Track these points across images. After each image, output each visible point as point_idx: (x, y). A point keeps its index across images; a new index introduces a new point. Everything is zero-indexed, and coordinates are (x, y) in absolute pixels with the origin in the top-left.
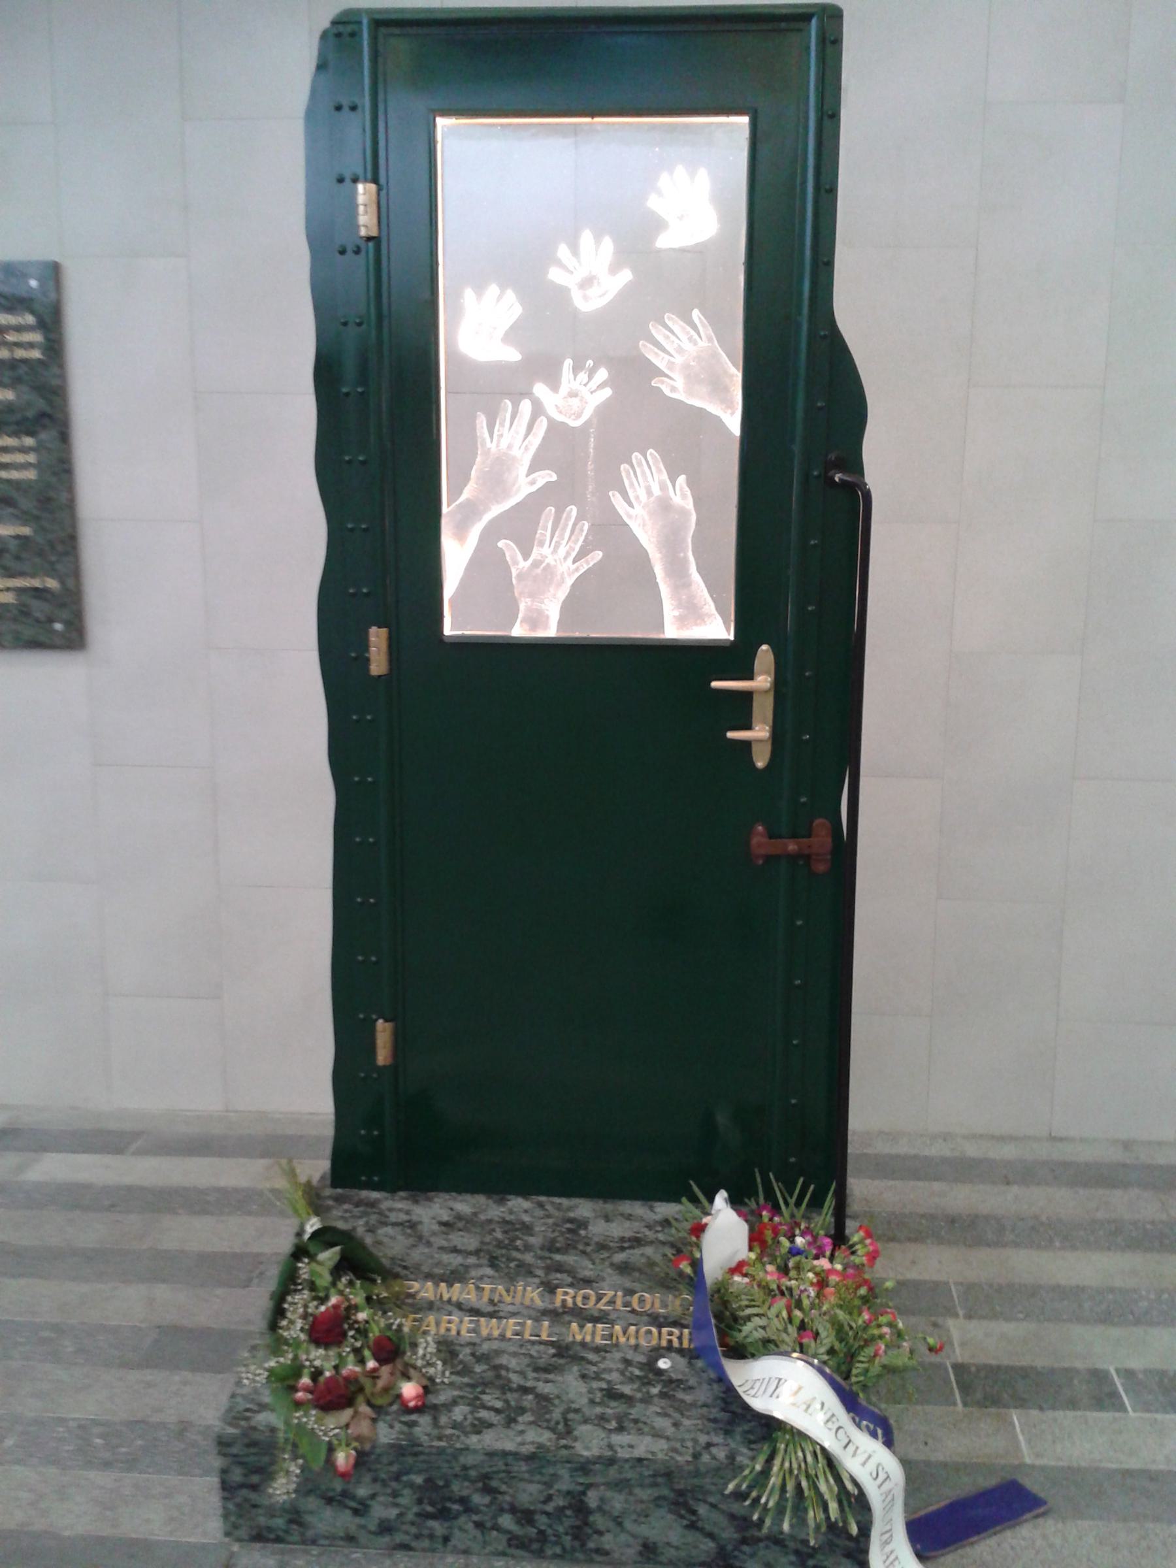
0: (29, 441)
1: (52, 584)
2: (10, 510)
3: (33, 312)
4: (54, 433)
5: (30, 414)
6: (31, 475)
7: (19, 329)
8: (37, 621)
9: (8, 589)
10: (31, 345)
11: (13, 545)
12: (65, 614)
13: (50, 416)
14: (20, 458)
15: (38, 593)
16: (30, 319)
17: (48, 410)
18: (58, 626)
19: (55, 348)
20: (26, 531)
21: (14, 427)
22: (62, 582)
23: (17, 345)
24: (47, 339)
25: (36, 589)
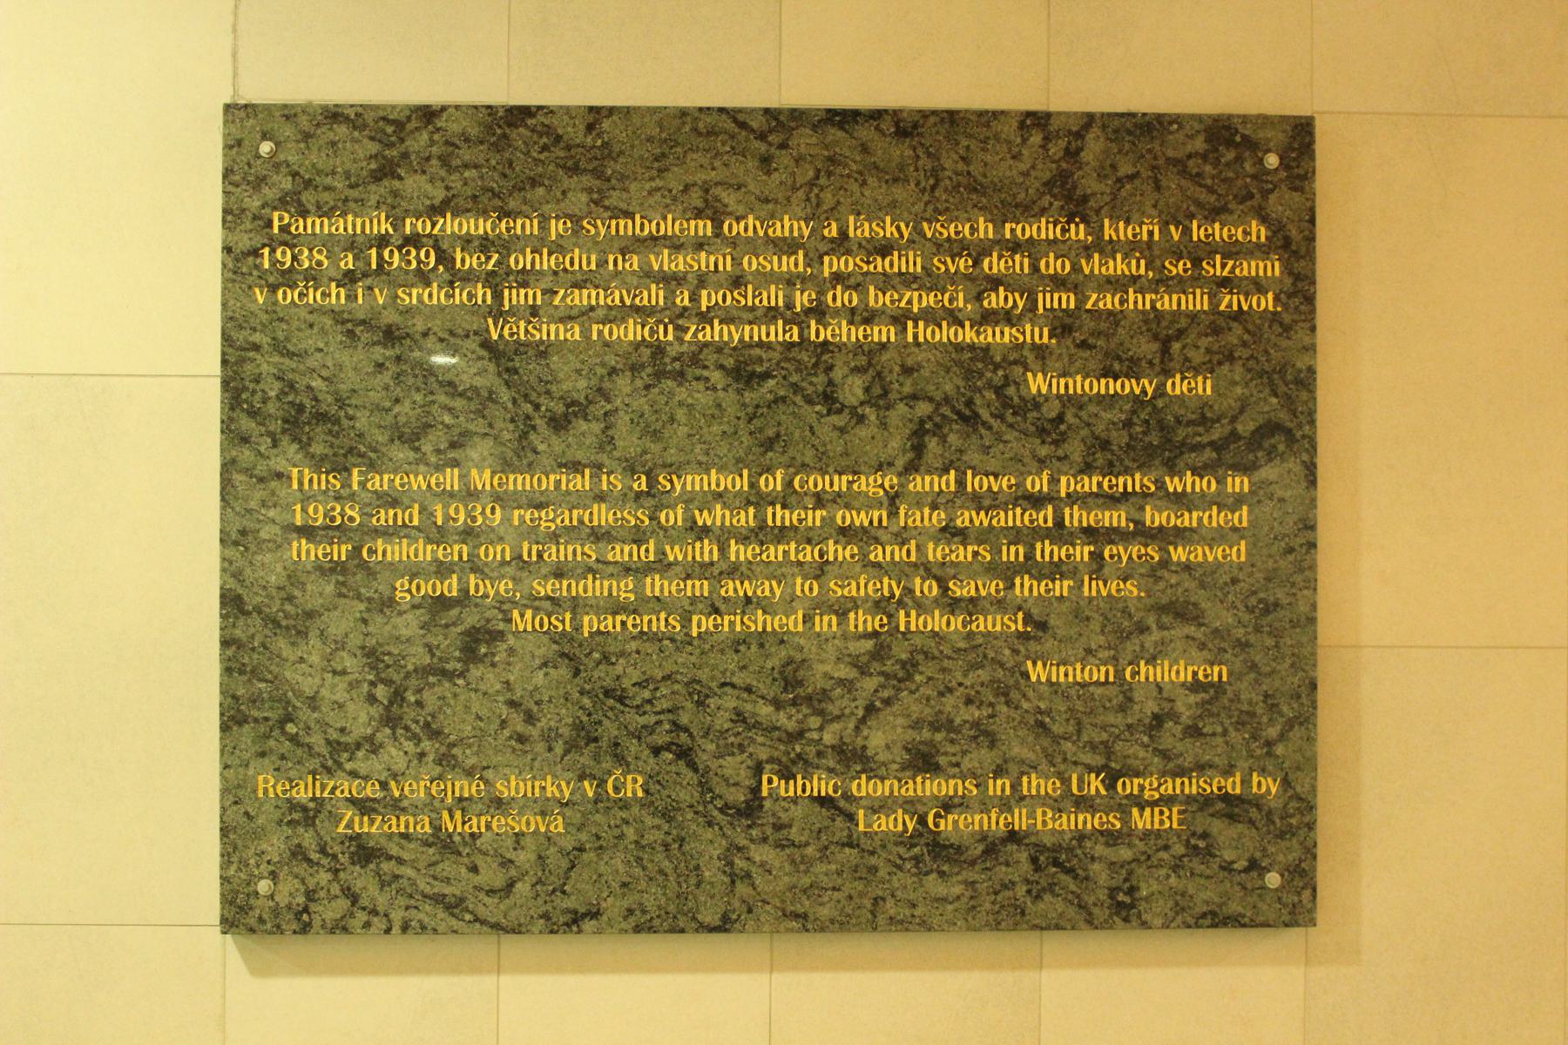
0: (1238, 483)
1: (1266, 786)
2: (1191, 630)
3: (1264, 220)
4: (1294, 465)
5: (1245, 427)
6: (1238, 553)
7: (1232, 251)
8: (1227, 867)
9: (1168, 801)
10: (1258, 286)
11: (1186, 706)
12: (1287, 852)
13: (1288, 432)
14: (1215, 518)
15: (1233, 807)
16: (1258, 231)
17: (1283, 416)
18: (1273, 879)
19: (1300, 290)
20: (1217, 672)
21: (1209, 454)
22: (1286, 783)
23: (1225, 283)
24: (1288, 270)
25: (1226, 798)
